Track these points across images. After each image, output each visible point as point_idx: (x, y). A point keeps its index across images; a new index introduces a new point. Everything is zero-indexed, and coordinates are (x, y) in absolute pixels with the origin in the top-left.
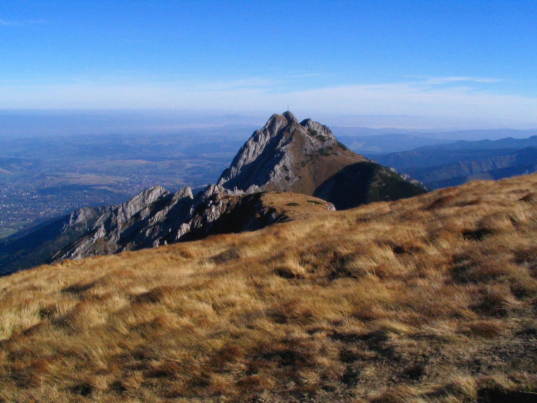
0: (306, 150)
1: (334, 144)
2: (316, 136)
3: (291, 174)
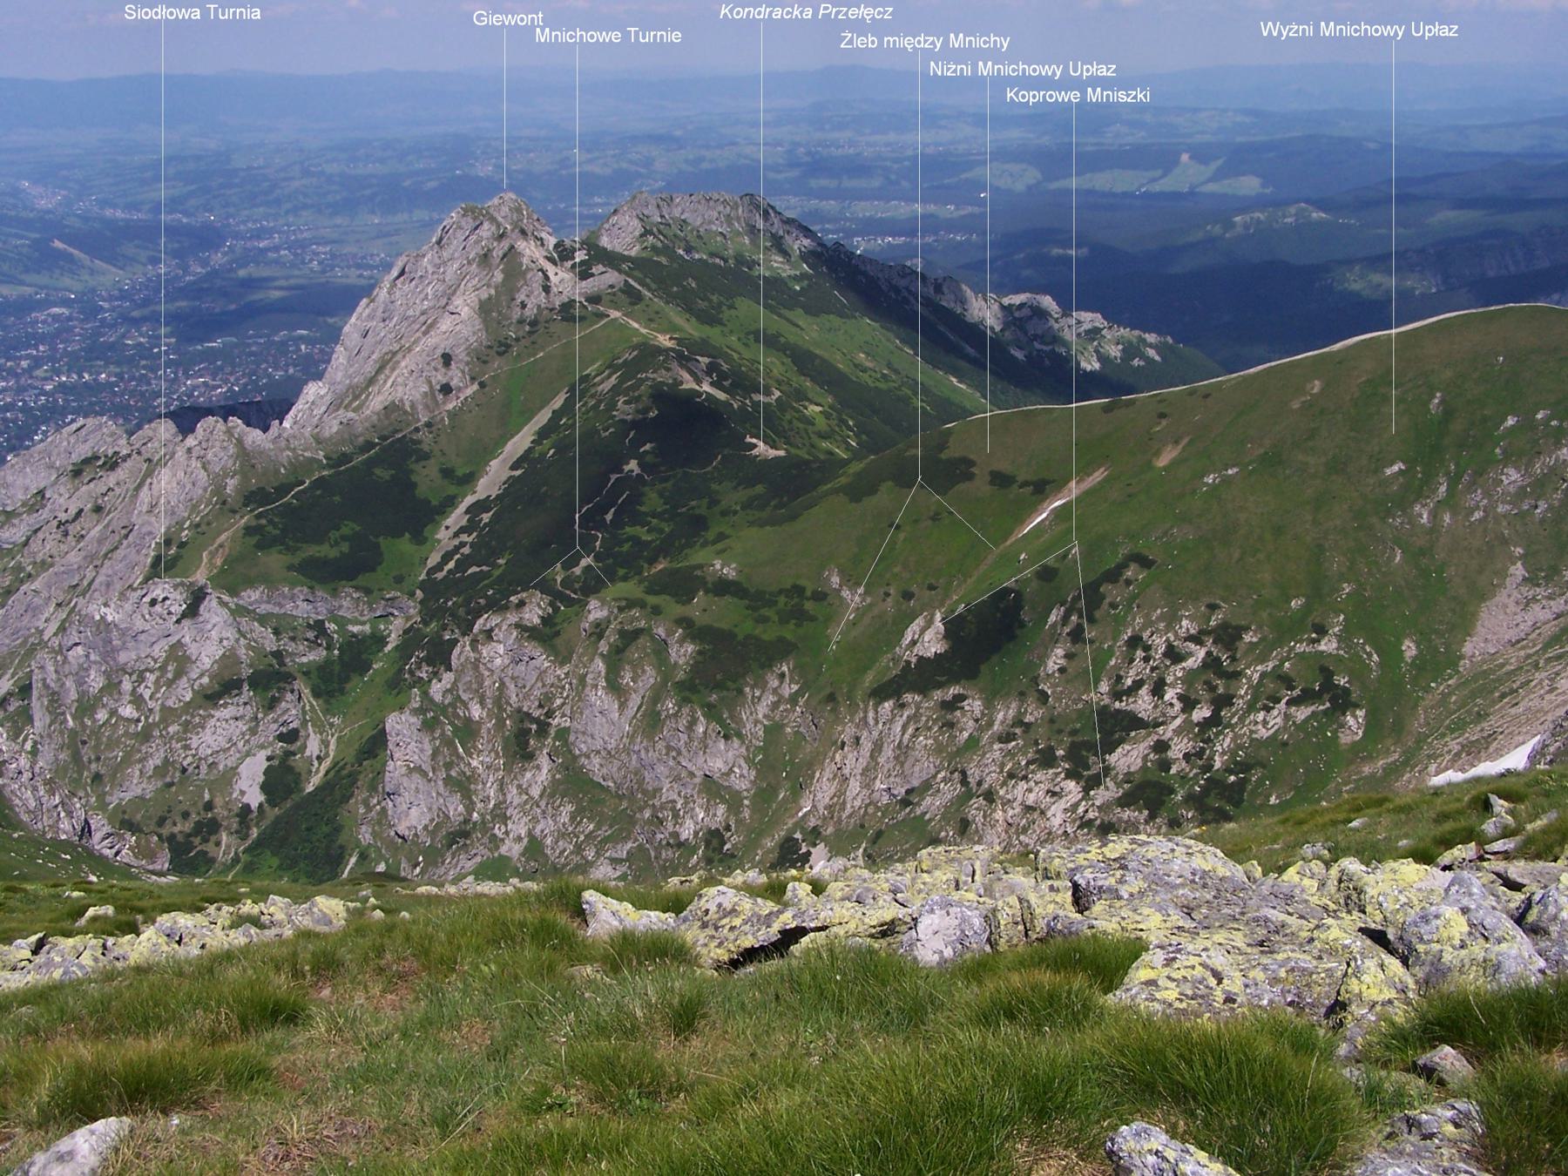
0: (523, 306)
1: (611, 286)
2: (570, 263)
3: (456, 376)
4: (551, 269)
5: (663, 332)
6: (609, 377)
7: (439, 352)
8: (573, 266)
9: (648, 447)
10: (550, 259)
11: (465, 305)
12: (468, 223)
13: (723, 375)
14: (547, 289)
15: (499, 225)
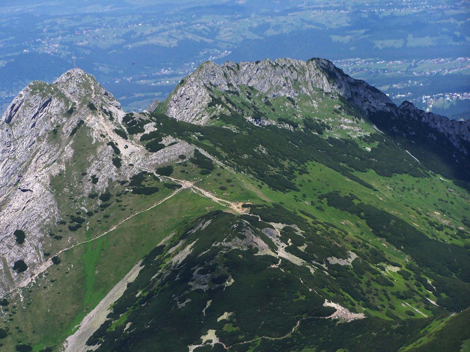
0: (95, 180)
1: (182, 157)
2: (140, 135)
4: (121, 143)
5: (236, 200)
6: (183, 247)
7: (12, 230)
8: (143, 139)
9: (225, 316)
10: (119, 132)
11: (36, 183)
12: (37, 101)
13: (298, 241)
14: (117, 162)
15: (67, 101)
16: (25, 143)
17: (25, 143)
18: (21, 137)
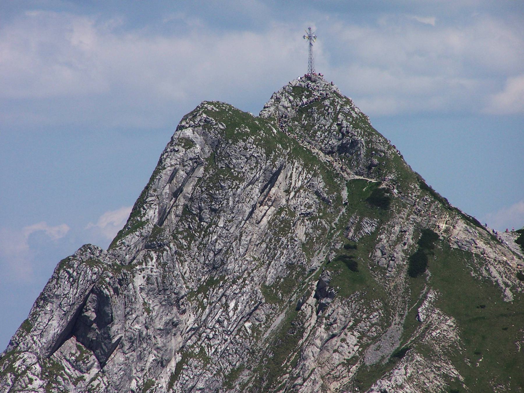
16: (232, 305)
17: (232, 305)
18: (211, 283)
